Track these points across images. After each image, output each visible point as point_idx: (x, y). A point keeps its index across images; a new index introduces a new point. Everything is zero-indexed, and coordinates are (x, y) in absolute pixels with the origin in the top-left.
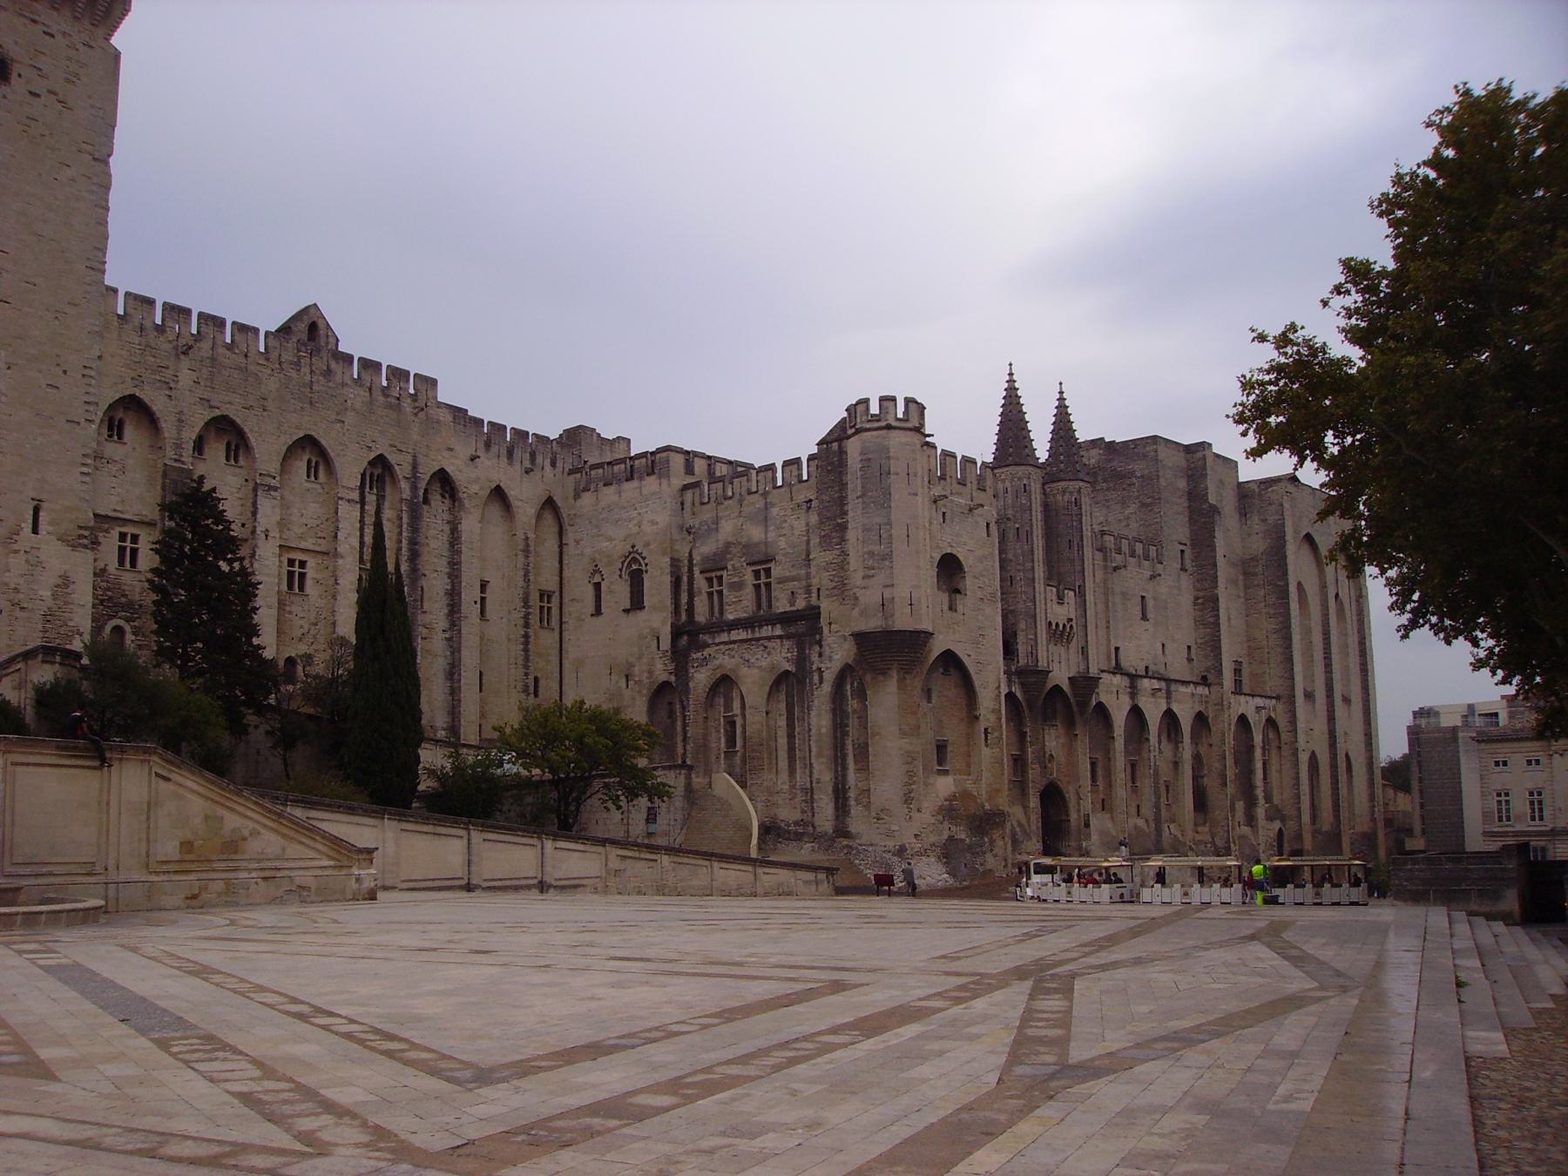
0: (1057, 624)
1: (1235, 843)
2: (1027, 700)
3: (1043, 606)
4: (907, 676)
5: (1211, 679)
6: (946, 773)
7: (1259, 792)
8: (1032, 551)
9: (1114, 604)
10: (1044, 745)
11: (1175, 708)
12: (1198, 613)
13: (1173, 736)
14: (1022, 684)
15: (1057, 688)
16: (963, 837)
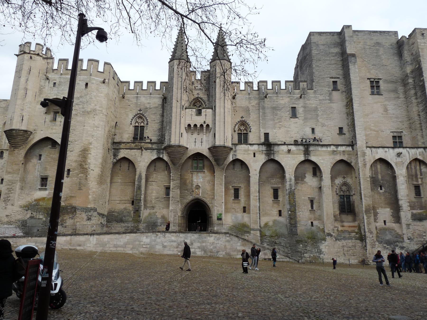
0: (195, 125)
1: (371, 233)
2: (171, 160)
3: (178, 118)
4: (16, 150)
5: (354, 143)
6: (46, 189)
7: (404, 203)
8: (172, 95)
9: (264, 113)
10: (192, 181)
11: (313, 158)
12: (348, 110)
13: (318, 174)
14: (169, 154)
15: (198, 156)
16: (41, 217)
